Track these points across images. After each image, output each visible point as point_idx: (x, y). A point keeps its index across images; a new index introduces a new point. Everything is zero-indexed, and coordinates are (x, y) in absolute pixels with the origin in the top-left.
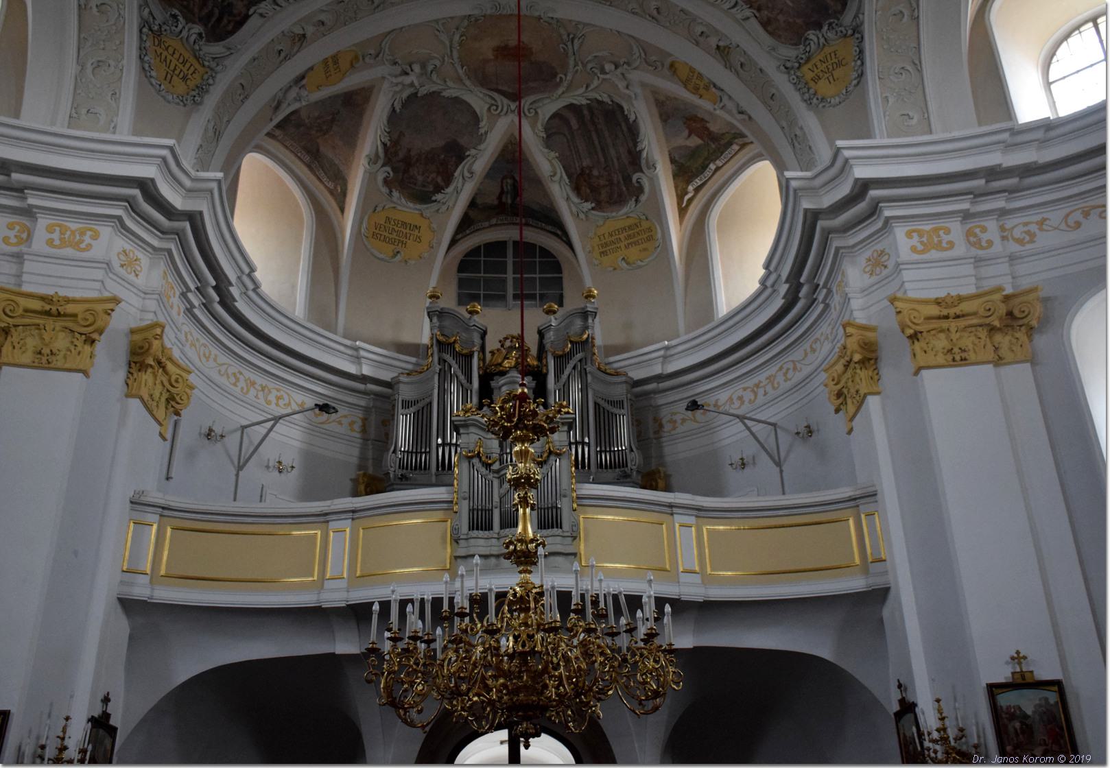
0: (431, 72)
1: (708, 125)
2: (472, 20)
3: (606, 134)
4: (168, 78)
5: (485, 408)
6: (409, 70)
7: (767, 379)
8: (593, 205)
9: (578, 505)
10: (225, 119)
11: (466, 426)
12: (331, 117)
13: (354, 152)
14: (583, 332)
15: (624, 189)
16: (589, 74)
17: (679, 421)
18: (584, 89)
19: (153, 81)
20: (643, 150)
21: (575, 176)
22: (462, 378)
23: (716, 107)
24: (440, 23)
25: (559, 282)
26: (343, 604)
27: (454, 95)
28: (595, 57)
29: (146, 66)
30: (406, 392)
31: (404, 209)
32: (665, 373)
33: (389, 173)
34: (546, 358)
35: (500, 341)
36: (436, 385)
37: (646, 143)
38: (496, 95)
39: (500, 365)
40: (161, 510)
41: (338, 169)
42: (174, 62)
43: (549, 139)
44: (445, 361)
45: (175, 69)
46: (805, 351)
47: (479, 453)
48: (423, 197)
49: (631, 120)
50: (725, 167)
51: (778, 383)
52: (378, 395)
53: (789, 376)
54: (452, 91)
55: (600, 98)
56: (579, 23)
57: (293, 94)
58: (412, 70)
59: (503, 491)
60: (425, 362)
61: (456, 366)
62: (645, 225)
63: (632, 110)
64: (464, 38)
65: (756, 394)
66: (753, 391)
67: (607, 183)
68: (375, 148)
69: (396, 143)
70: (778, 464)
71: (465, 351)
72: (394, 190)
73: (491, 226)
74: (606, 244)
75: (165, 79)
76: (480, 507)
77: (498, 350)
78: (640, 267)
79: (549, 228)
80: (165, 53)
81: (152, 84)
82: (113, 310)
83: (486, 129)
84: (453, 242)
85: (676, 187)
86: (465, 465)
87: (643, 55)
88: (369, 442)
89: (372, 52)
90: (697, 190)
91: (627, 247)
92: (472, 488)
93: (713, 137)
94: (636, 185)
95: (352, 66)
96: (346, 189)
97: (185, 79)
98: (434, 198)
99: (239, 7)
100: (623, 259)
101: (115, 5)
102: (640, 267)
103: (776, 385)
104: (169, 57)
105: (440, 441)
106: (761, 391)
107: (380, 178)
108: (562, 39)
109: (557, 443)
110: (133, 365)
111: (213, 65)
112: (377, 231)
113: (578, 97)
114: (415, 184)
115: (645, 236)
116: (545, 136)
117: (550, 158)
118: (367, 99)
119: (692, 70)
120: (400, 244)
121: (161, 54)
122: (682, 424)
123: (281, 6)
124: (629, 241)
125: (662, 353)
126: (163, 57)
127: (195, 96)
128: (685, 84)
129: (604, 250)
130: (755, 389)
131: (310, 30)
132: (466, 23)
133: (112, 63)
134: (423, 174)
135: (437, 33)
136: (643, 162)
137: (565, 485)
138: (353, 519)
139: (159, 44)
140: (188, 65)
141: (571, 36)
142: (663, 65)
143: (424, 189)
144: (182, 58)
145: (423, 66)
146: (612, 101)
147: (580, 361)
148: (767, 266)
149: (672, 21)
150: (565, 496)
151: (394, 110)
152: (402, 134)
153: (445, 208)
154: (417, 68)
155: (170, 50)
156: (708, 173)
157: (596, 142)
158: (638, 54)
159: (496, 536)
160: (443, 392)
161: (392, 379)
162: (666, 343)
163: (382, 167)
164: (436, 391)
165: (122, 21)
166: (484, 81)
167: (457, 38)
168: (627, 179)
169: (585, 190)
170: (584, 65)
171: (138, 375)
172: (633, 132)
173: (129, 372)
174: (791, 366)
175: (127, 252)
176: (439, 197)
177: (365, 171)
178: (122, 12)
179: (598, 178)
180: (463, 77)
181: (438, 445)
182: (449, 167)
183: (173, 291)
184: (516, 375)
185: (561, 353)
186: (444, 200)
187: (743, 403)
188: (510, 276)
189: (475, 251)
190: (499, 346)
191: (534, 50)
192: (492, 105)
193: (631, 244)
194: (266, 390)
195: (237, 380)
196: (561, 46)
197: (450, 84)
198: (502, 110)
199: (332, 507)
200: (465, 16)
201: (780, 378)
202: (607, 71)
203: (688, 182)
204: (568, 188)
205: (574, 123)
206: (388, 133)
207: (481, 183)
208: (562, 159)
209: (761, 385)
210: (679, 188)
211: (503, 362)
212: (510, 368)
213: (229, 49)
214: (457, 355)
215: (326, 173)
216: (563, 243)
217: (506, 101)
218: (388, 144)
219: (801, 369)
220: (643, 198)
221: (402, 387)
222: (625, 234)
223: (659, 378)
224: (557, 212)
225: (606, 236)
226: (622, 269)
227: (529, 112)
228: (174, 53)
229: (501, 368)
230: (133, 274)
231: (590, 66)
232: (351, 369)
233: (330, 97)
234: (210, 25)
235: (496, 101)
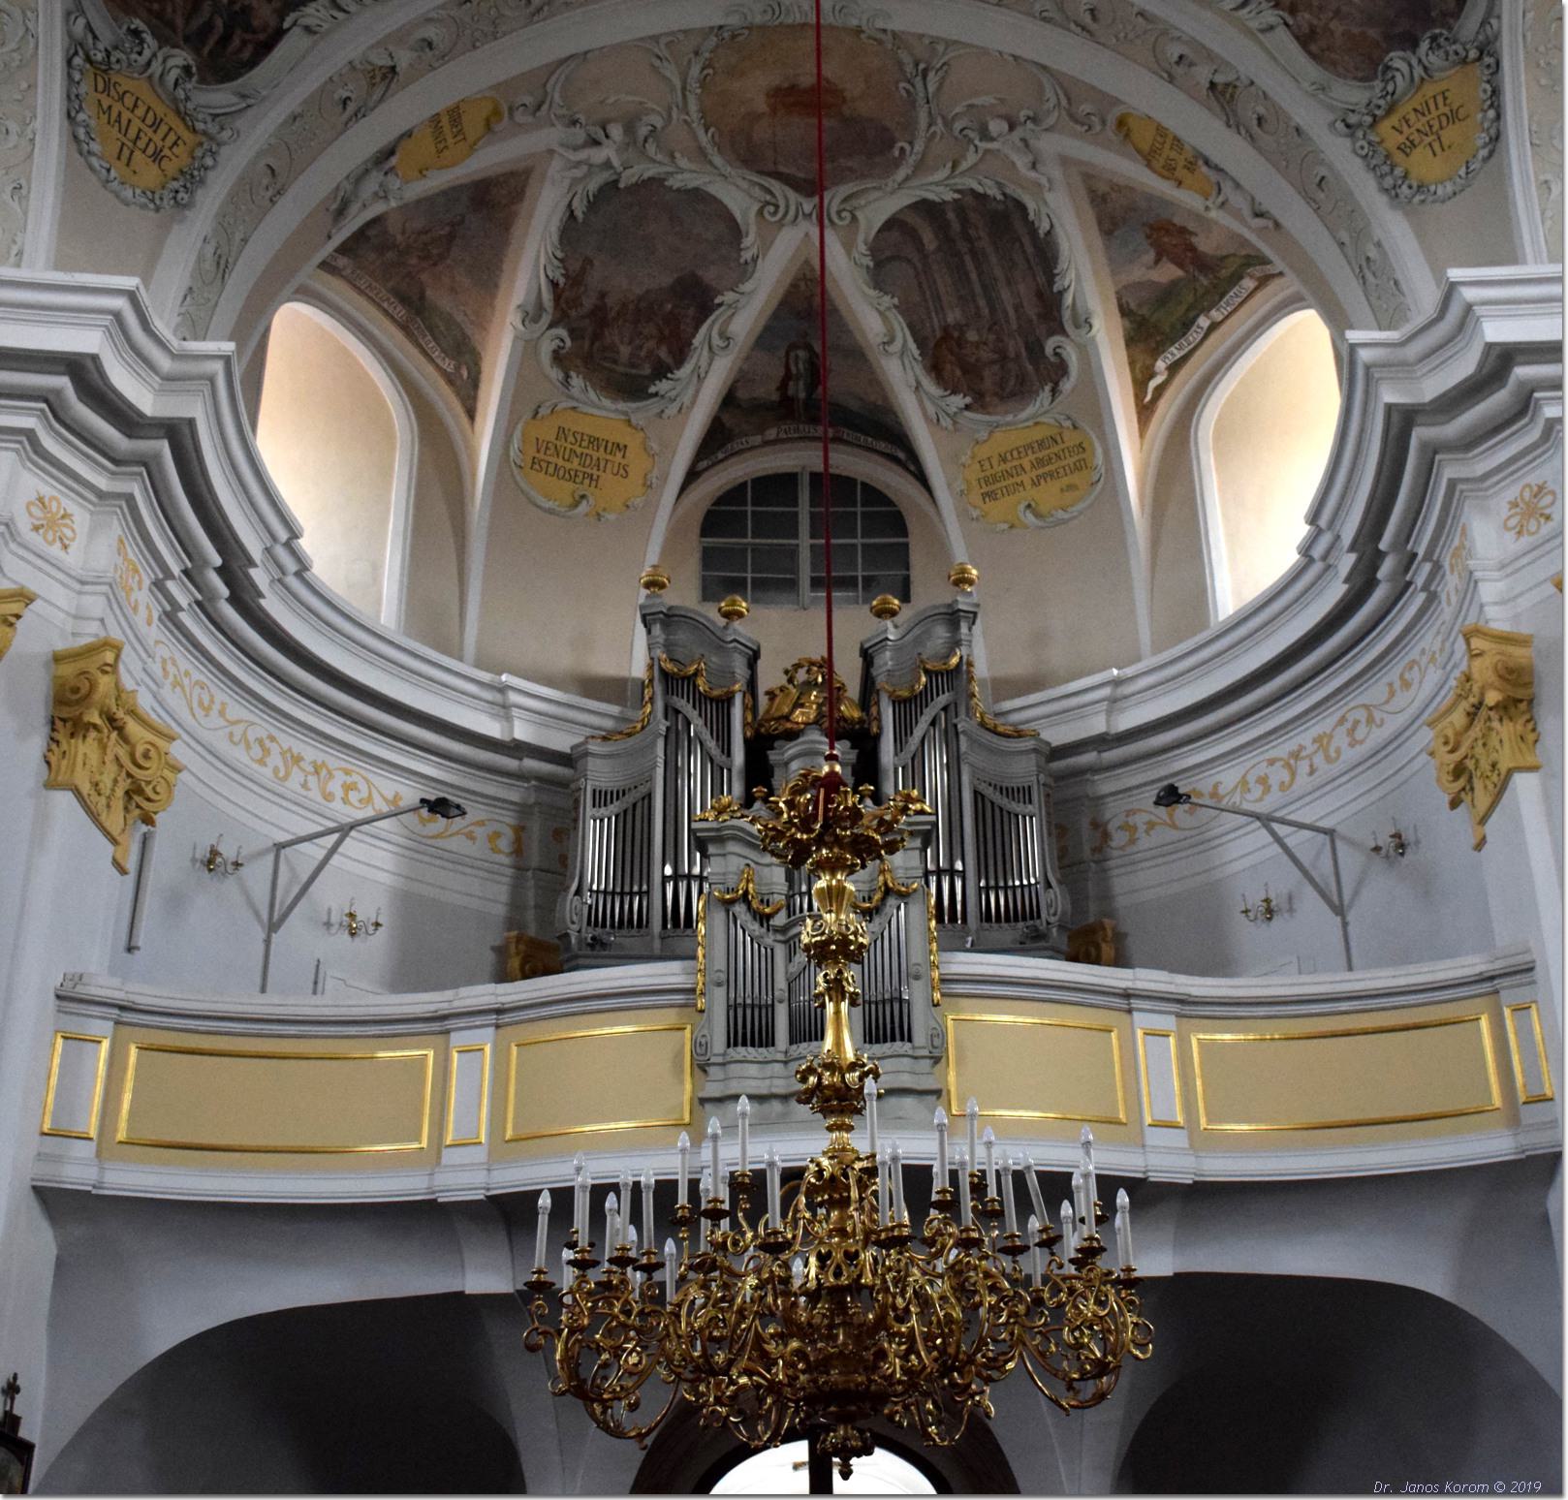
0: (645, 141)
1: (1194, 240)
2: (726, 35)
3: (993, 259)
4: (124, 155)
5: (757, 805)
7: (1315, 741)
8: (968, 400)
9: (943, 995)
10: (238, 236)
11: (720, 840)
12: (448, 228)
13: (493, 296)
14: (951, 653)
15: (1030, 368)
16: (956, 138)
17: (1142, 828)
18: (946, 172)
19: (94, 161)
20: (1066, 290)
21: (932, 345)
22: (711, 744)
23: (1209, 203)
24: (663, 41)
25: (900, 556)
26: (479, 1196)
28: (971, 106)
29: (81, 132)
30: (600, 774)
31: (591, 410)
32: (1113, 731)
33: (562, 340)
34: (877, 703)
35: (786, 672)
36: (660, 761)
37: (1071, 274)
38: (776, 186)
39: (787, 718)
40: (117, 1011)
41: (465, 336)
42: (136, 124)
43: (879, 274)
44: (677, 712)
45: (138, 137)
46: (1390, 685)
47: (746, 893)
48: (632, 388)
49: (1042, 232)
50: (1229, 322)
51: (1338, 751)
52: (544, 780)
53: (1360, 733)
54: (687, 176)
55: (980, 190)
56: (935, 40)
57: (371, 185)
58: (607, 136)
59: (794, 968)
60: (639, 715)
61: (700, 722)
62: (1071, 439)
63: (1044, 210)
64: (711, 71)
65: (1293, 774)
66: (1288, 765)
67: (996, 356)
68: (533, 296)
69: (576, 279)
70: (1339, 910)
71: (716, 693)
73: (766, 443)
74: (994, 476)
75: (119, 158)
76: (749, 1001)
77: (782, 689)
78: (1064, 522)
79: (882, 446)
80: (117, 107)
81: (91, 168)
82: (18, 617)
83: (754, 251)
84: (692, 476)
85: (1132, 363)
86: (719, 917)
88: (530, 874)
89: (528, 100)
90: (1174, 369)
91: (1035, 484)
92: (732, 965)
93: (1201, 263)
94: (1053, 359)
95: (488, 126)
96: (479, 372)
97: (157, 157)
98: (652, 389)
99: (264, 14)
100: (1029, 506)
101: (17, 13)
102: (1064, 522)
103: (1333, 755)
104: (126, 115)
105: (668, 871)
106: (1303, 767)
107: (547, 347)
108: (902, 70)
109: (900, 873)
110: (59, 724)
111: (212, 128)
112: (541, 456)
113: (937, 187)
114: (615, 362)
115: (1071, 461)
116: (871, 264)
117: (882, 308)
120: (587, 481)
121: (110, 107)
122: (1147, 832)
123: (345, 11)
124: (1040, 471)
125: (1106, 692)
126: (114, 115)
127: (177, 192)
129: (993, 487)
130: (1292, 762)
131: (404, 59)
132: (713, 41)
133: (13, 127)
134: (630, 343)
135: (657, 63)
136: (1067, 315)
137: (917, 956)
138: (498, 1027)
139: (106, 89)
140: (163, 129)
141: (922, 66)
142: (1104, 122)
143: (634, 371)
144: (151, 115)
145: (630, 129)
146: (1004, 194)
147: (945, 709)
148: (1313, 518)
150: (917, 977)
152: (588, 262)
153: (672, 410)
154: (616, 131)
155: (129, 101)
156: (1194, 336)
157: (974, 276)
158: (1053, 101)
159: (781, 1057)
160: (673, 772)
161: (572, 748)
162: (1115, 672)
164: (660, 771)
165: (32, 45)
166: (750, 156)
167: (695, 71)
168: (1035, 350)
169: (953, 370)
170: (948, 124)
171: (69, 743)
172: (1045, 255)
173: (52, 739)
174: (1362, 715)
175: (46, 501)
176: (662, 386)
177: (516, 338)
178: (30, 25)
179: (977, 345)
180: (710, 150)
181: (665, 879)
183: (137, 578)
184: (817, 738)
185: (905, 694)
186: (673, 394)
187: (1267, 789)
188: (805, 542)
189: (734, 495)
190: (783, 680)
191: (847, 94)
192: (768, 203)
193: (1044, 476)
194: (324, 772)
195: (266, 752)
196: (902, 85)
197: (683, 163)
198: (786, 213)
199: (456, 1004)
200: (712, 28)
201: (1341, 739)
202: (994, 134)
203: (1156, 352)
204: (919, 370)
205: (929, 239)
206: (561, 261)
207: (747, 358)
208: (904, 309)
209: (1303, 754)
210: (1138, 366)
211: (792, 711)
212: (807, 724)
213: (244, 97)
214: (700, 700)
216: (910, 478)
217: (792, 196)
218: (562, 281)
219: (1382, 720)
220: (1067, 386)
221: (592, 764)
222: (1032, 457)
223: (1103, 741)
224: (895, 414)
225: (995, 462)
226: (1026, 527)
227: (841, 218)
228: (136, 105)
229: (789, 725)
230: (58, 544)
231: (958, 126)
232: (492, 728)
234: (206, 50)
235: (771, 193)
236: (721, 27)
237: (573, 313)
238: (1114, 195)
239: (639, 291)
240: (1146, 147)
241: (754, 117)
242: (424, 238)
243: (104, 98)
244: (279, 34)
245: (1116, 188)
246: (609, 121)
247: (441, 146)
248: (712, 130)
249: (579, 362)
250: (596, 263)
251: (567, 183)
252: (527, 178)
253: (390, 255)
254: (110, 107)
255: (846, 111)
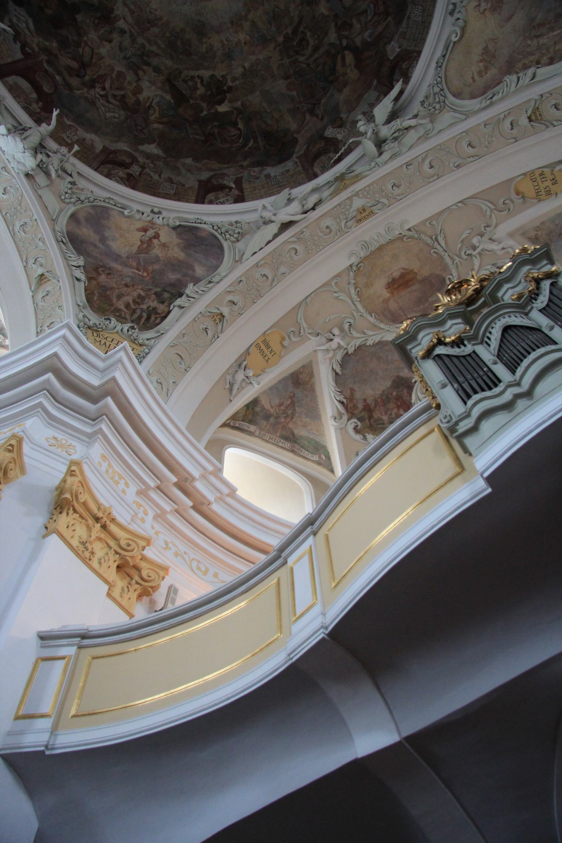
0: (350, 330)
2: (354, 268)
6: (332, 337)
13: (321, 421)
16: (466, 259)
24: (333, 284)
27: (377, 340)
28: (462, 241)
41: (317, 442)
54: (374, 337)
56: (430, 220)
58: (334, 335)
64: (358, 289)
69: (351, 398)
72: (367, 435)
87: (492, 207)
99: (162, 308)
107: (350, 427)
108: (428, 245)
118: (311, 375)
119: (530, 175)
121: (100, 341)
123: (194, 298)
128: (539, 198)
131: (225, 311)
132: (352, 274)
134: (386, 414)
135: (336, 295)
139: (98, 336)
141: (434, 237)
145: (342, 330)
149: (487, 143)
151: (337, 374)
152: (352, 390)
154: (336, 331)
163: (348, 421)
167: (352, 291)
170: (459, 257)
177: (336, 430)
180: (377, 323)
182: (405, 398)
191: (416, 271)
196: (432, 251)
197: (370, 333)
200: (348, 269)
213: (158, 332)
215: (308, 451)
233: (280, 382)
236: (351, 266)
237: (356, 412)
238: (539, 233)
239: (379, 393)
240: (534, 195)
241: (386, 301)
242: (282, 408)
243: (98, 339)
244: (169, 312)
245: (537, 229)
246: (332, 329)
247: (266, 358)
248: (373, 315)
249: (367, 430)
250: (356, 389)
251: (328, 361)
252: (312, 367)
253: (272, 420)
254: (100, 341)
255: (419, 278)
